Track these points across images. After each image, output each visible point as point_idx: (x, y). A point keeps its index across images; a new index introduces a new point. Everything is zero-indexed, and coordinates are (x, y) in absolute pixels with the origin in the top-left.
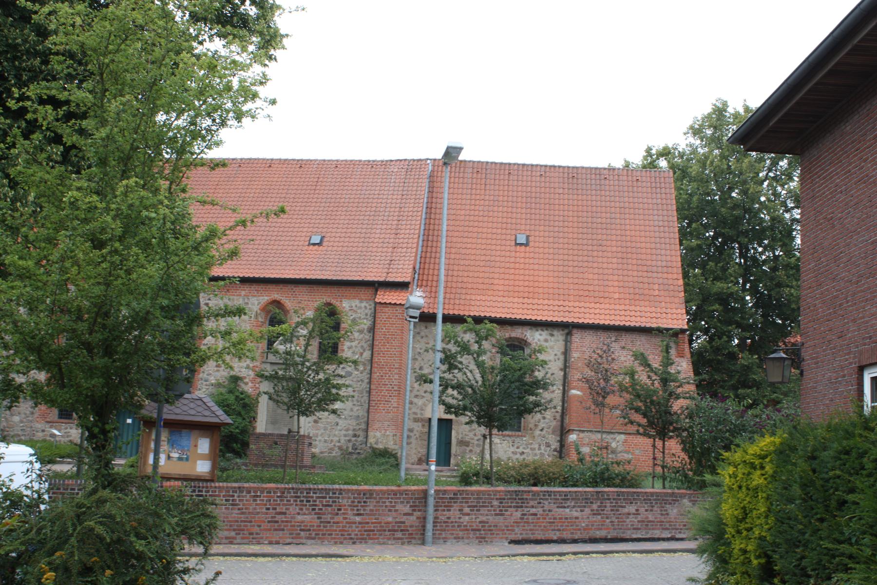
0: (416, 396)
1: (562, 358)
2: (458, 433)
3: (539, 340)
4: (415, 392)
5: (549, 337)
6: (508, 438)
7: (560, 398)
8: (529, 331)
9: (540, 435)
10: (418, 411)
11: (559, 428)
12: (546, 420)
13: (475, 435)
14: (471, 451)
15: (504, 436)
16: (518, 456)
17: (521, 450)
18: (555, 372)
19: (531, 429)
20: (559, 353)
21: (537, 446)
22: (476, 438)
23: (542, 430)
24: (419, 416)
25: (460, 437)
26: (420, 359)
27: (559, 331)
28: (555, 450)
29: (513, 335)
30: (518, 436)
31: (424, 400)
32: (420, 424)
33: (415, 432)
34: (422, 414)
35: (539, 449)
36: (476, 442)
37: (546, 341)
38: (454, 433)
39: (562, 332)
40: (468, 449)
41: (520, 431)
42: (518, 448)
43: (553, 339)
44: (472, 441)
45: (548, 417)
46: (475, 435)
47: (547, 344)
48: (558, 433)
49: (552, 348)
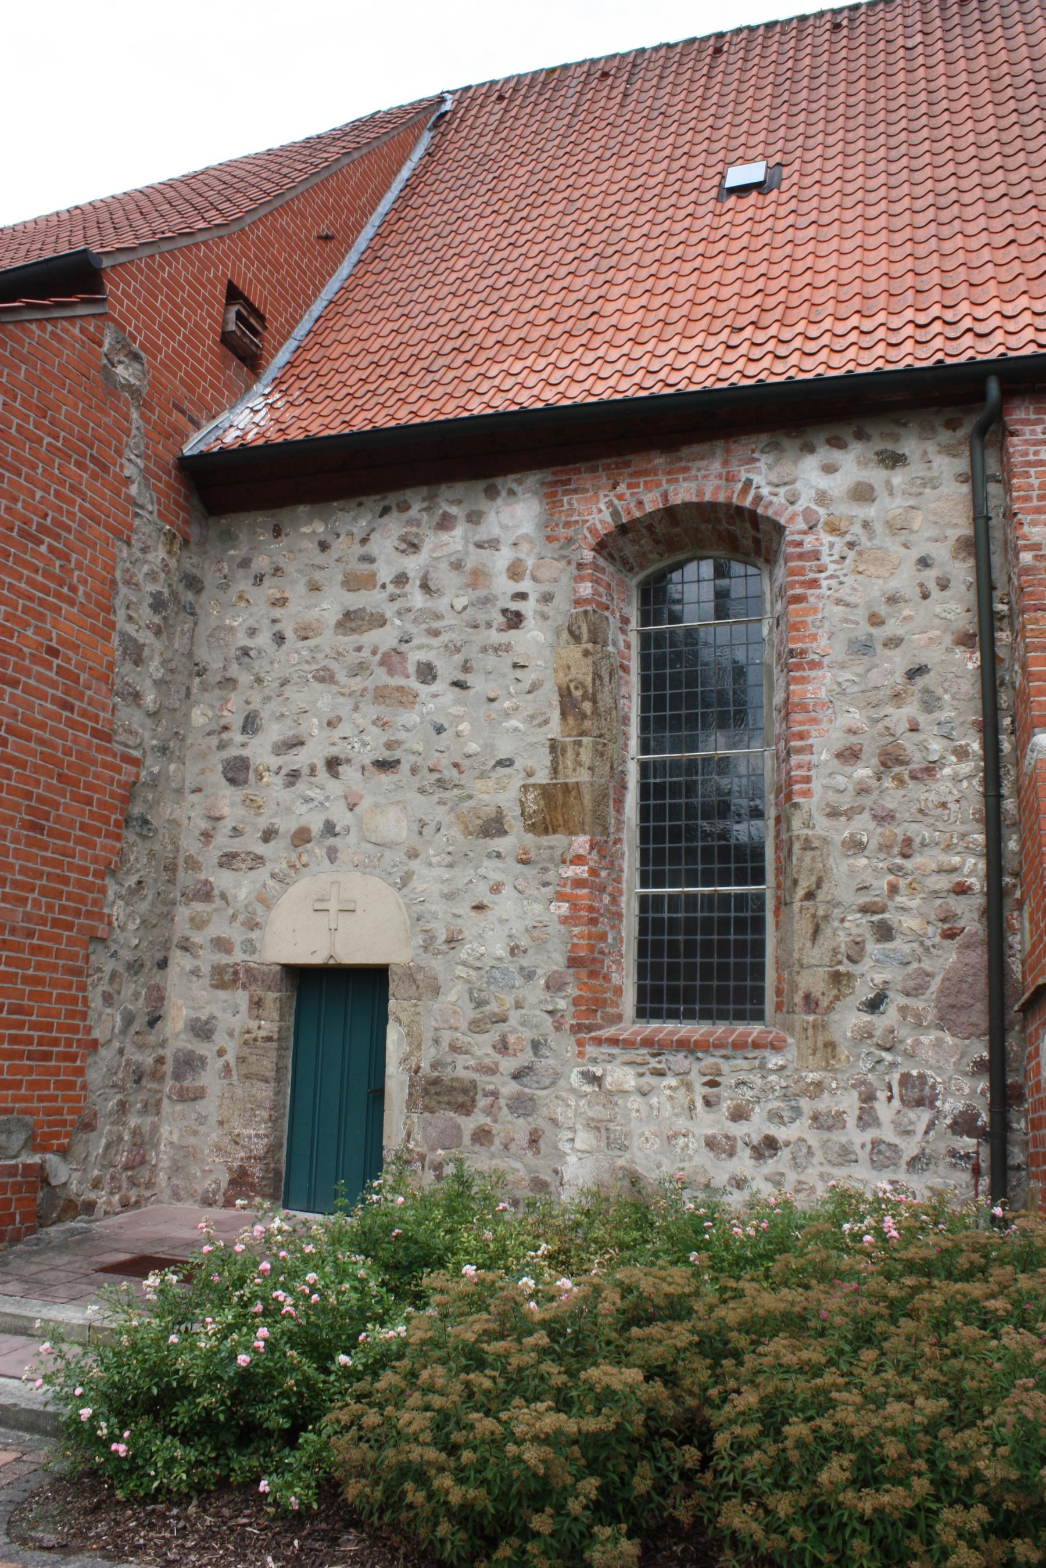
0: (228, 860)
1: (962, 572)
2: (414, 1038)
3: (822, 498)
4: (223, 842)
5: (876, 476)
6: (679, 1060)
7: (974, 804)
8: (764, 461)
9: (866, 1034)
10: (236, 934)
11: (981, 985)
12: (899, 945)
13: (503, 1047)
14: (483, 1136)
15: (656, 1046)
16: (743, 1163)
17: (756, 1128)
18: (932, 657)
19: (810, 1002)
20: (941, 552)
21: (849, 1103)
22: (508, 1064)
23: (874, 1005)
24: (238, 956)
25: (427, 1056)
26: (245, 678)
27: (927, 431)
28: (964, 1124)
29: (683, 492)
30: (739, 1045)
31: (262, 874)
32: (242, 997)
33: (220, 1039)
34: (250, 947)
35: (867, 1119)
36: (510, 1088)
37: (863, 494)
38: (393, 1035)
39: (945, 436)
40: (469, 1124)
41: (758, 1016)
42: (739, 1115)
43: (898, 477)
44: (485, 1082)
45: (909, 923)
46: (503, 1047)
47: (870, 512)
48: (979, 1015)
49: (897, 528)
